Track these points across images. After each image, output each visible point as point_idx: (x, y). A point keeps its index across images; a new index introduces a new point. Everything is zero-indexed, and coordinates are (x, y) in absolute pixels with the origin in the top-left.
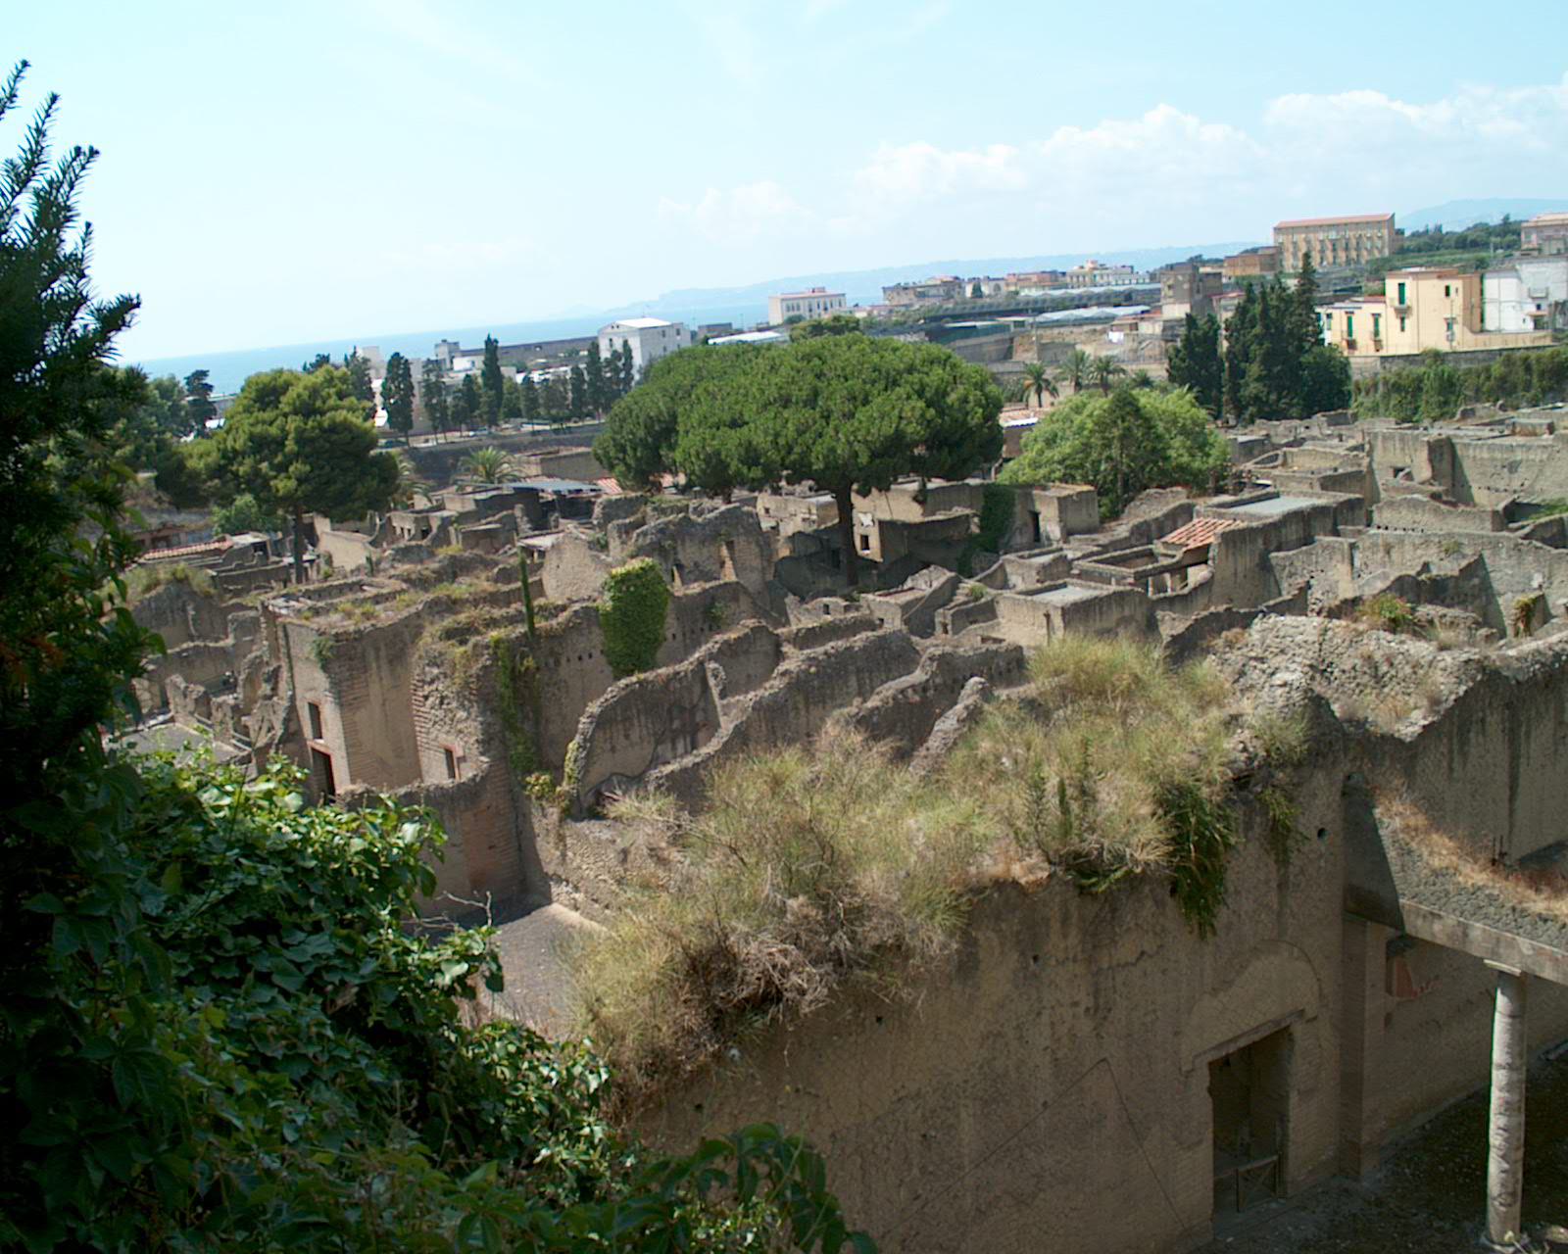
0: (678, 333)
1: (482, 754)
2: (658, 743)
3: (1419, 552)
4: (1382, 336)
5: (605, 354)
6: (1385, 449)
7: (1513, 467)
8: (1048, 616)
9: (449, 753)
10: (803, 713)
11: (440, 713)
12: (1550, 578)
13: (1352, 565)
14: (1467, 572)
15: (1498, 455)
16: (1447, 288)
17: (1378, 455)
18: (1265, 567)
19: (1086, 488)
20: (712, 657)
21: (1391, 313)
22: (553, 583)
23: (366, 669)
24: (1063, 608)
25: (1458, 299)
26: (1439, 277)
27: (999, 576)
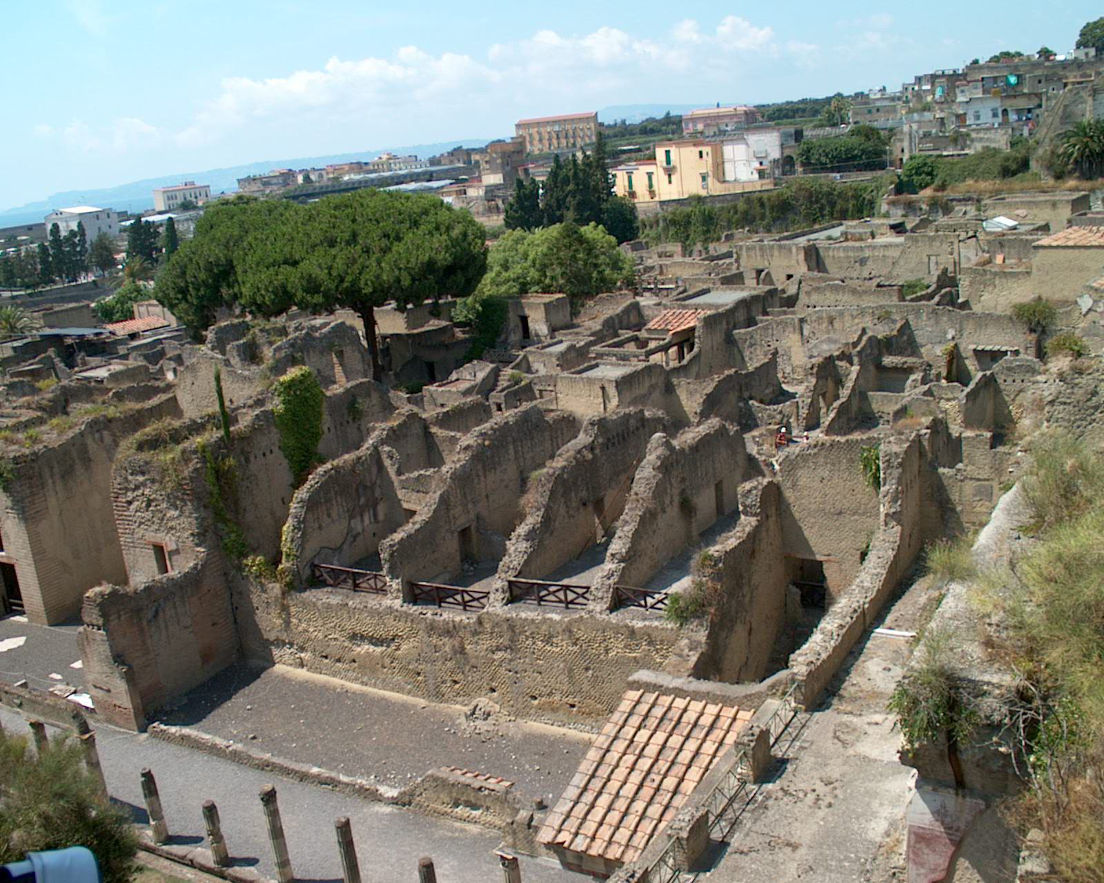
0: (109, 216)
1: (197, 545)
2: (351, 517)
3: (857, 321)
4: (655, 187)
5: (64, 233)
6: (748, 257)
7: (863, 262)
8: (603, 388)
9: (159, 550)
10: (482, 479)
11: (148, 515)
12: (961, 331)
13: (802, 334)
14: (901, 331)
15: (851, 254)
16: (701, 153)
17: (743, 262)
18: (730, 341)
19: (560, 296)
20: (383, 442)
21: (661, 171)
22: (188, 397)
23: (43, 485)
24: (616, 381)
25: (708, 159)
26: (695, 145)
27: (524, 365)
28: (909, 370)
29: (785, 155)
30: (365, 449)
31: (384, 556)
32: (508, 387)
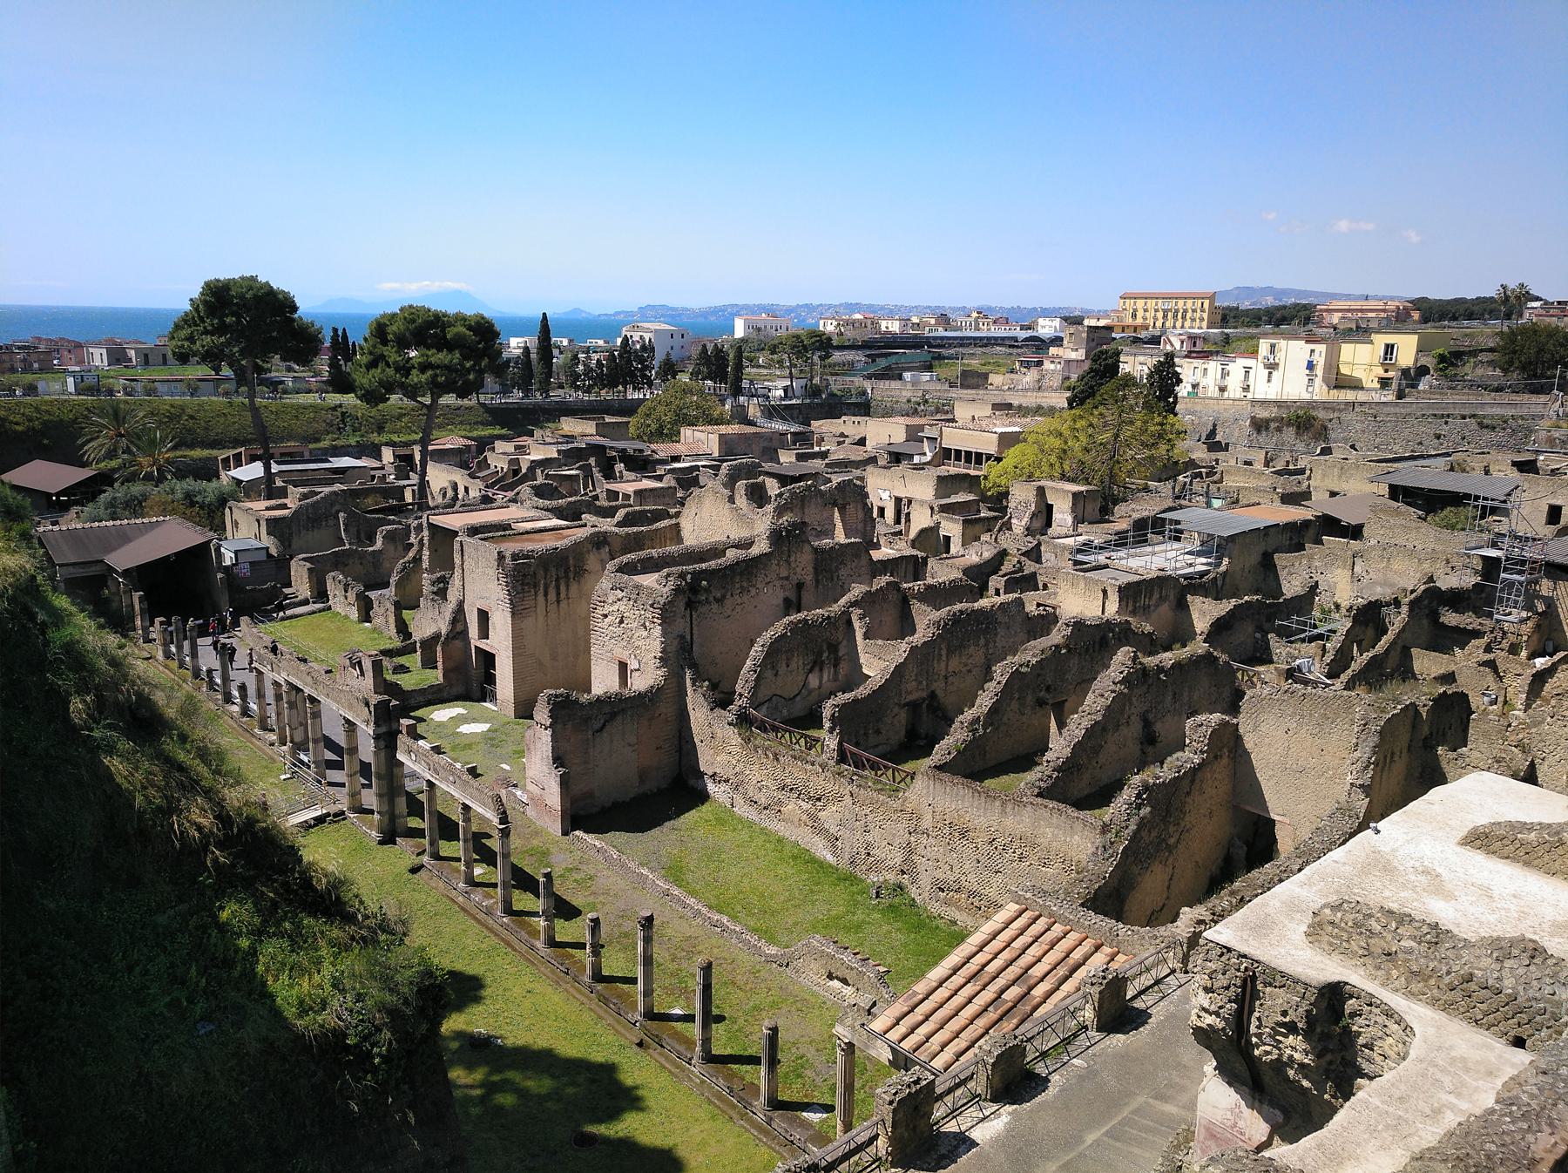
9: (623, 666)
11: (619, 631)
20: (854, 604)
28: (1477, 634)
29: (1419, 365)
30: (837, 607)
31: (827, 713)
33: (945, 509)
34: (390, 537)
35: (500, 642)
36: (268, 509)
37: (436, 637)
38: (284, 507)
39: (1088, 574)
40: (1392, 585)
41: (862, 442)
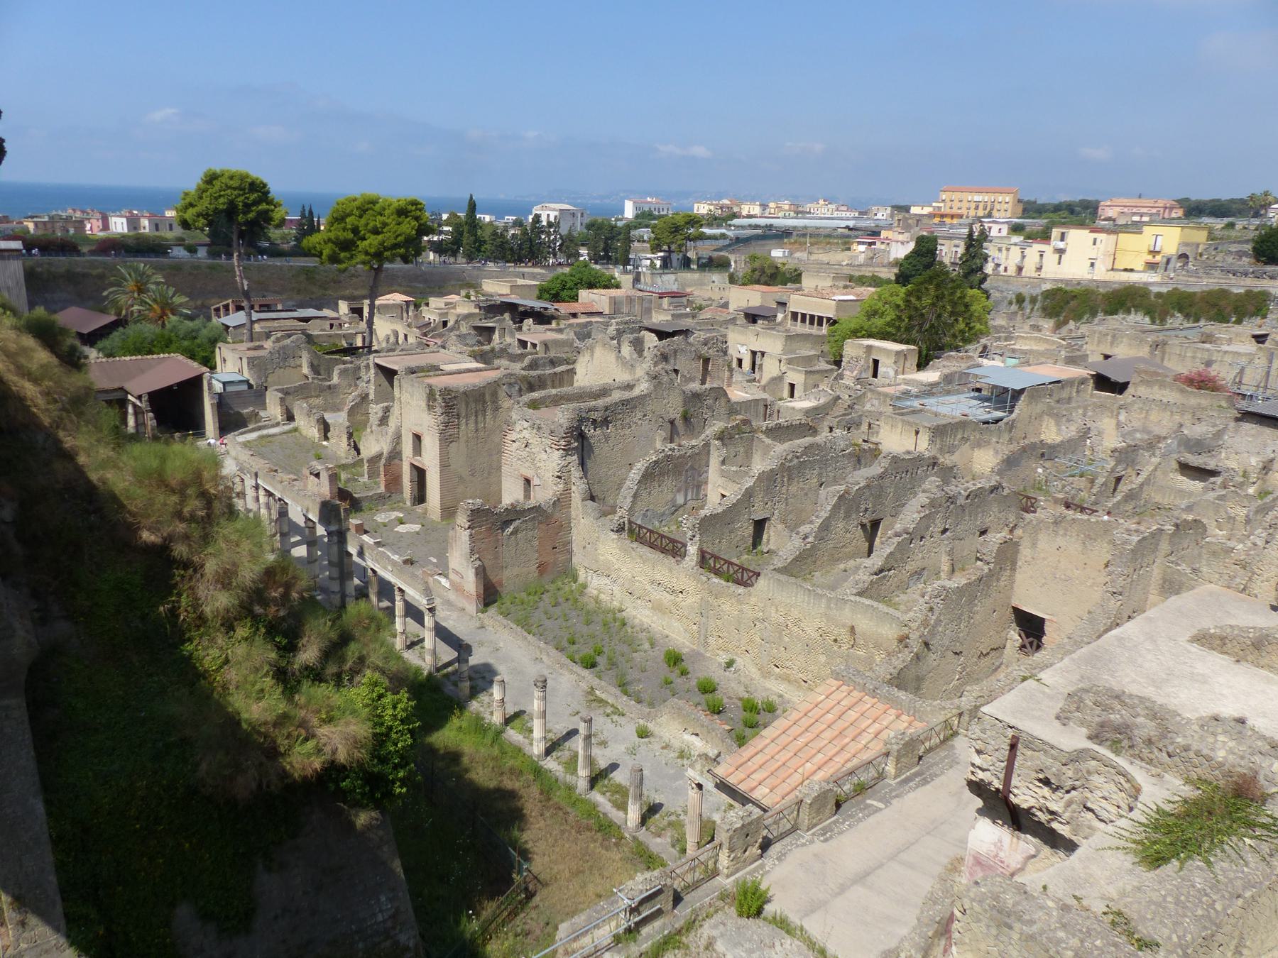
2: (679, 491)
11: (524, 454)
32: (844, 415)
33: (790, 362)
34: (343, 373)
35: (430, 460)
36: (249, 349)
37: (379, 456)
38: (261, 347)
39: (905, 418)
40: (1149, 432)
41: (726, 305)
